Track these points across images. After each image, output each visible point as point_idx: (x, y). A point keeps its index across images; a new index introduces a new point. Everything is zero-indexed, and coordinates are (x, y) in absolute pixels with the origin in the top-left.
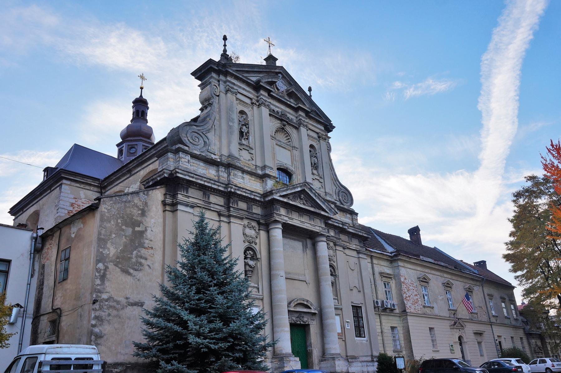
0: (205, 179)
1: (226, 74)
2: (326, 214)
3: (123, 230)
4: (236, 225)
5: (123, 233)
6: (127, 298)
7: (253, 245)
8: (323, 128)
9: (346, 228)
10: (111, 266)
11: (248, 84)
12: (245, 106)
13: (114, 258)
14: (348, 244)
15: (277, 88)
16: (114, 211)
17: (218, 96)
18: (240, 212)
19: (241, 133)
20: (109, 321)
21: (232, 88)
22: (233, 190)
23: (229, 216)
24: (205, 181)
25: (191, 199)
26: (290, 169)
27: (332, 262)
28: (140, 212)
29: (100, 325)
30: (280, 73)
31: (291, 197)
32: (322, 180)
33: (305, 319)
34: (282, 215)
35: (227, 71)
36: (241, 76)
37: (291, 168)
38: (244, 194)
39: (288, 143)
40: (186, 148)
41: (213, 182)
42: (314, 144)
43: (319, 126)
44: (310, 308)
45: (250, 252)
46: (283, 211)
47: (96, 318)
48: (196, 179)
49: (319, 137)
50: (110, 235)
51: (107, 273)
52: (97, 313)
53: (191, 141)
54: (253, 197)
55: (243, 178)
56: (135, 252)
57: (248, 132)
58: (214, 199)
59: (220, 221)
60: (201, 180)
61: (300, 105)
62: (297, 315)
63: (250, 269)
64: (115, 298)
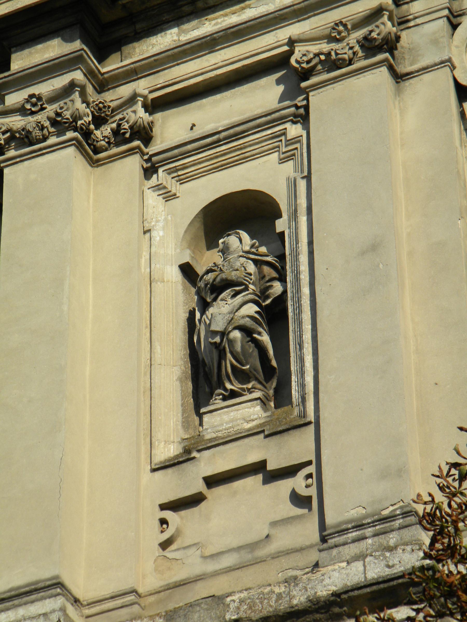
32: (277, 454)
42: (264, 174)
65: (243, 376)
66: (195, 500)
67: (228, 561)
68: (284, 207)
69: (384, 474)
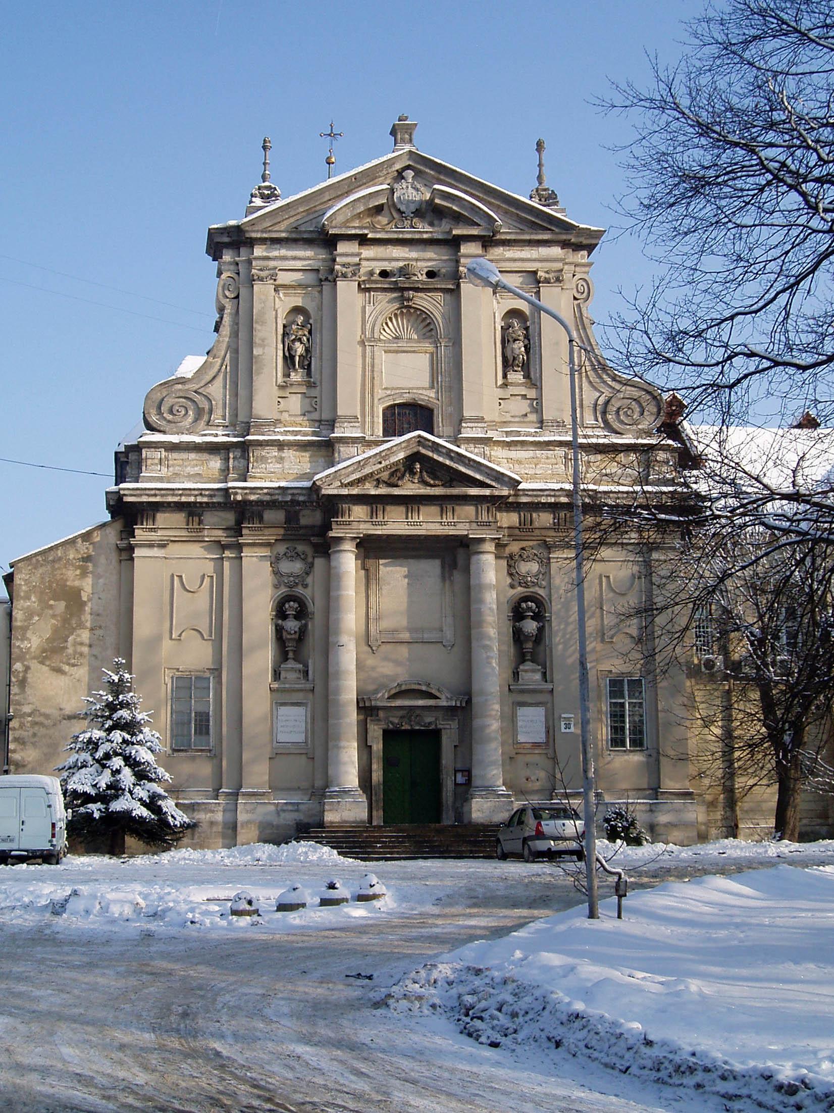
3: (51, 607)
5: (51, 612)
6: (61, 709)
7: (300, 590)
8: (556, 251)
10: (34, 665)
13: (38, 652)
15: (399, 211)
16: (35, 580)
20: (34, 744)
25: (160, 533)
26: (423, 400)
27: (536, 589)
28: (78, 572)
29: (22, 750)
30: (408, 167)
33: (428, 720)
37: (428, 396)
39: (429, 334)
43: (544, 251)
44: (436, 698)
45: (292, 603)
47: (16, 740)
51: (28, 675)
52: (17, 734)
55: (281, 460)
56: (70, 638)
61: (454, 232)
62: (401, 713)
63: (289, 637)
64: (43, 710)
67: (517, 419)
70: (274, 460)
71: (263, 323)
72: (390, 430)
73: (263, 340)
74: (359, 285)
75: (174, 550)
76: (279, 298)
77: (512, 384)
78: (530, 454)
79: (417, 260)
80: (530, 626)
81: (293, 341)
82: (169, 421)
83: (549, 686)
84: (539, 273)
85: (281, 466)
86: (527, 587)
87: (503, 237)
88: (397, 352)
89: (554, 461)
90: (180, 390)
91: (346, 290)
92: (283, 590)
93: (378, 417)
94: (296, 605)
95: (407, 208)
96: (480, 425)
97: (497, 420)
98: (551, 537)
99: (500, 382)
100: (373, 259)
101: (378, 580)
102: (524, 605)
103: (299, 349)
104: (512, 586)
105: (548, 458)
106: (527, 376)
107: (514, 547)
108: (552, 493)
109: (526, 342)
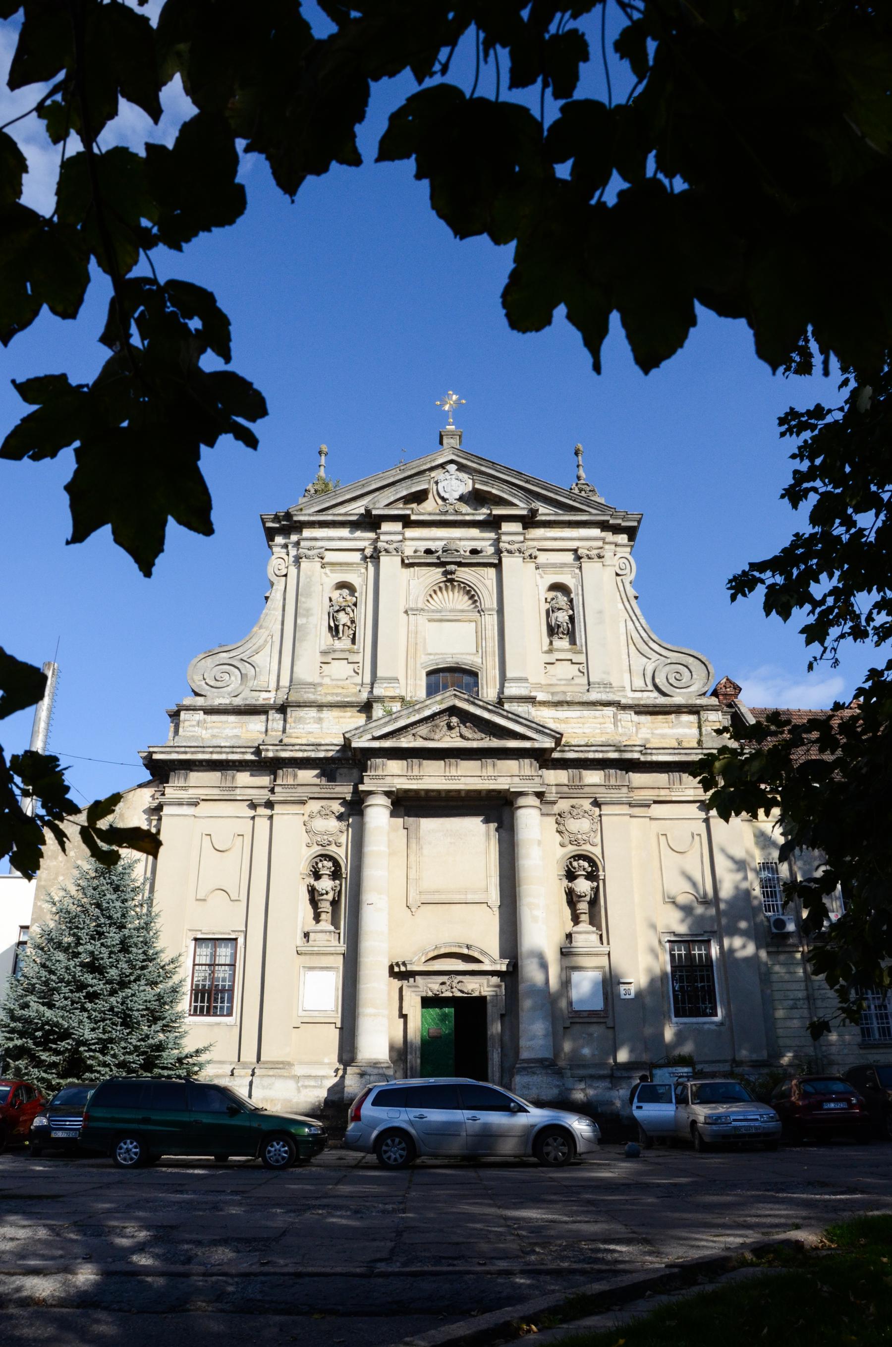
0: (211, 750)
1: (299, 527)
2: (527, 744)
4: (286, 817)
7: (333, 848)
8: (596, 532)
9: (636, 756)
11: (354, 525)
12: (346, 572)
14: (663, 792)
15: (444, 499)
17: (286, 575)
18: (300, 789)
19: (334, 631)
21: (313, 548)
22: (270, 754)
23: (269, 805)
24: (211, 753)
25: (191, 791)
27: (588, 847)
31: (423, 730)
34: (394, 775)
35: (299, 522)
36: (330, 518)
38: (300, 755)
40: (200, 701)
41: (227, 750)
44: (478, 961)
46: (394, 766)
48: (193, 753)
49: (578, 558)
50: (56, 878)
53: (212, 683)
54: (321, 755)
57: (353, 622)
58: (243, 778)
59: (253, 818)
60: (203, 752)
61: (495, 512)
65: (563, 634)
66: (553, 664)
67: (563, 682)
68: (573, 590)
69: (604, 673)
70: (312, 721)
71: (309, 595)
72: (432, 690)
73: (308, 610)
74: (403, 561)
75: (204, 809)
76: (326, 574)
77: (557, 650)
78: (578, 714)
79: (460, 539)
80: (583, 886)
81: (338, 611)
82: (212, 687)
83: (605, 949)
84: (580, 552)
85: (319, 726)
86: (578, 845)
87: (544, 518)
88: (441, 621)
89: (602, 720)
90: (224, 658)
91: (389, 563)
92: (316, 850)
93: (421, 680)
94: (330, 864)
95: (451, 495)
96: (523, 685)
97: (543, 682)
98: (603, 795)
99: (546, 647)
100: (417, 540)
101: (418, 839)
102: (575, 864)
103: (343, 618)
104: (562, 845)
105: (595, 718)
106: (573, 642)
107: (563, 805)
108: (600, 748)
109: (571, 612)
